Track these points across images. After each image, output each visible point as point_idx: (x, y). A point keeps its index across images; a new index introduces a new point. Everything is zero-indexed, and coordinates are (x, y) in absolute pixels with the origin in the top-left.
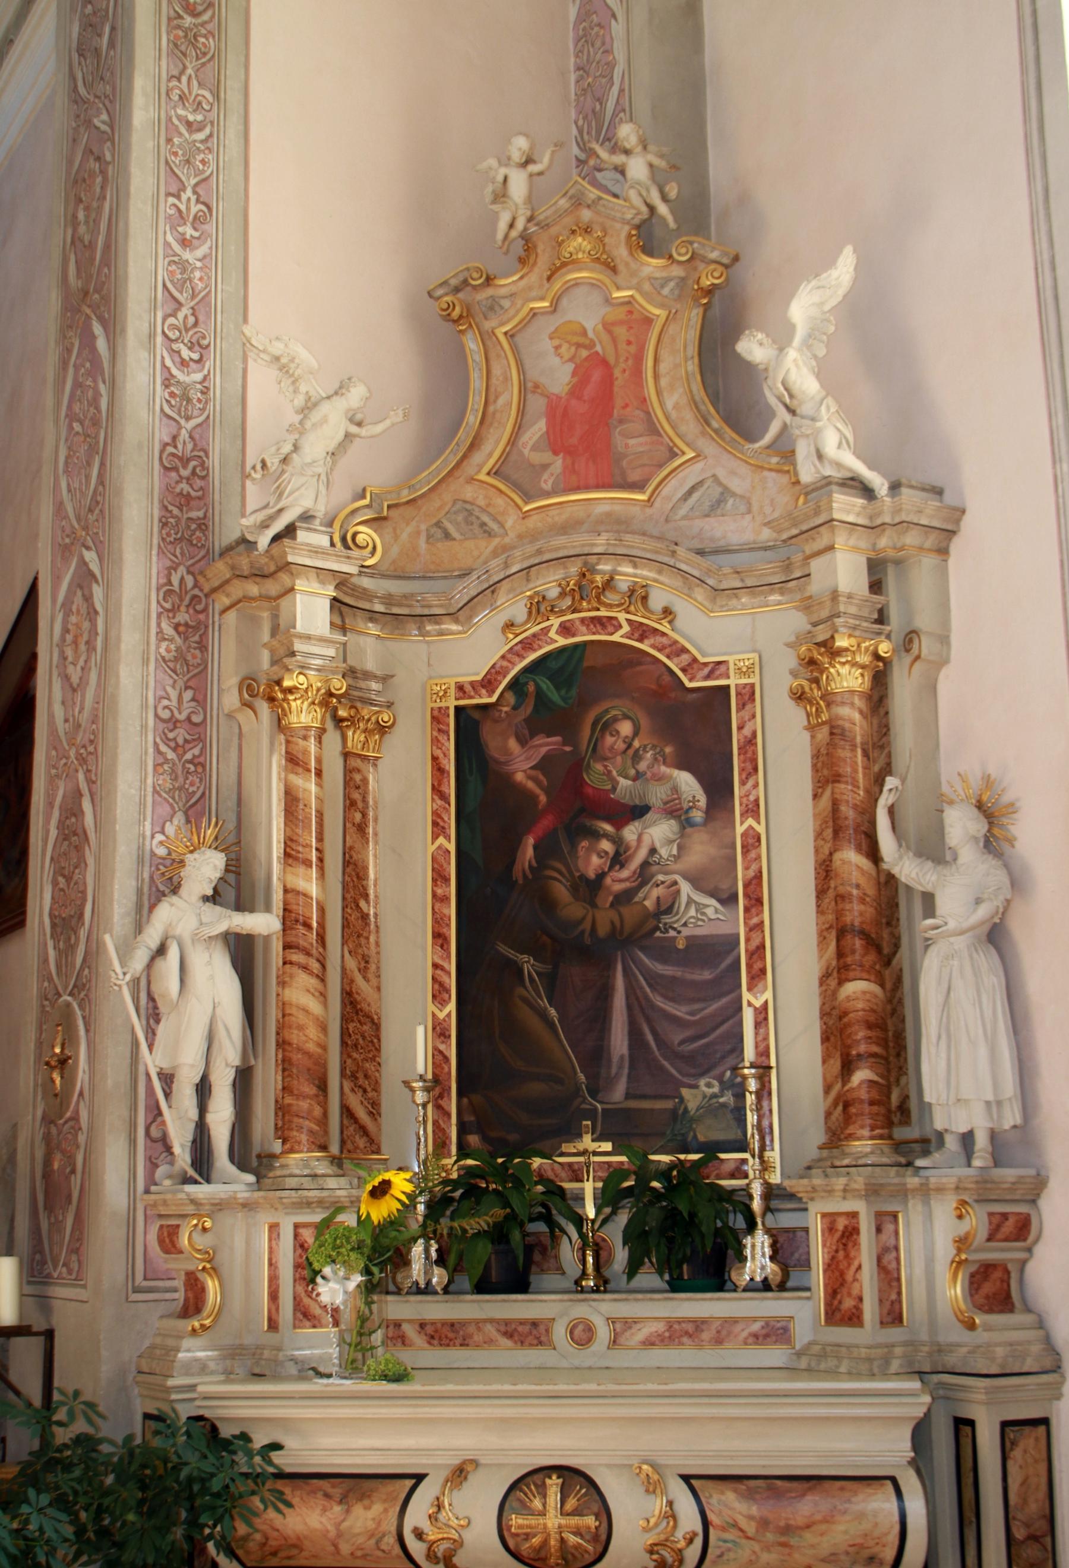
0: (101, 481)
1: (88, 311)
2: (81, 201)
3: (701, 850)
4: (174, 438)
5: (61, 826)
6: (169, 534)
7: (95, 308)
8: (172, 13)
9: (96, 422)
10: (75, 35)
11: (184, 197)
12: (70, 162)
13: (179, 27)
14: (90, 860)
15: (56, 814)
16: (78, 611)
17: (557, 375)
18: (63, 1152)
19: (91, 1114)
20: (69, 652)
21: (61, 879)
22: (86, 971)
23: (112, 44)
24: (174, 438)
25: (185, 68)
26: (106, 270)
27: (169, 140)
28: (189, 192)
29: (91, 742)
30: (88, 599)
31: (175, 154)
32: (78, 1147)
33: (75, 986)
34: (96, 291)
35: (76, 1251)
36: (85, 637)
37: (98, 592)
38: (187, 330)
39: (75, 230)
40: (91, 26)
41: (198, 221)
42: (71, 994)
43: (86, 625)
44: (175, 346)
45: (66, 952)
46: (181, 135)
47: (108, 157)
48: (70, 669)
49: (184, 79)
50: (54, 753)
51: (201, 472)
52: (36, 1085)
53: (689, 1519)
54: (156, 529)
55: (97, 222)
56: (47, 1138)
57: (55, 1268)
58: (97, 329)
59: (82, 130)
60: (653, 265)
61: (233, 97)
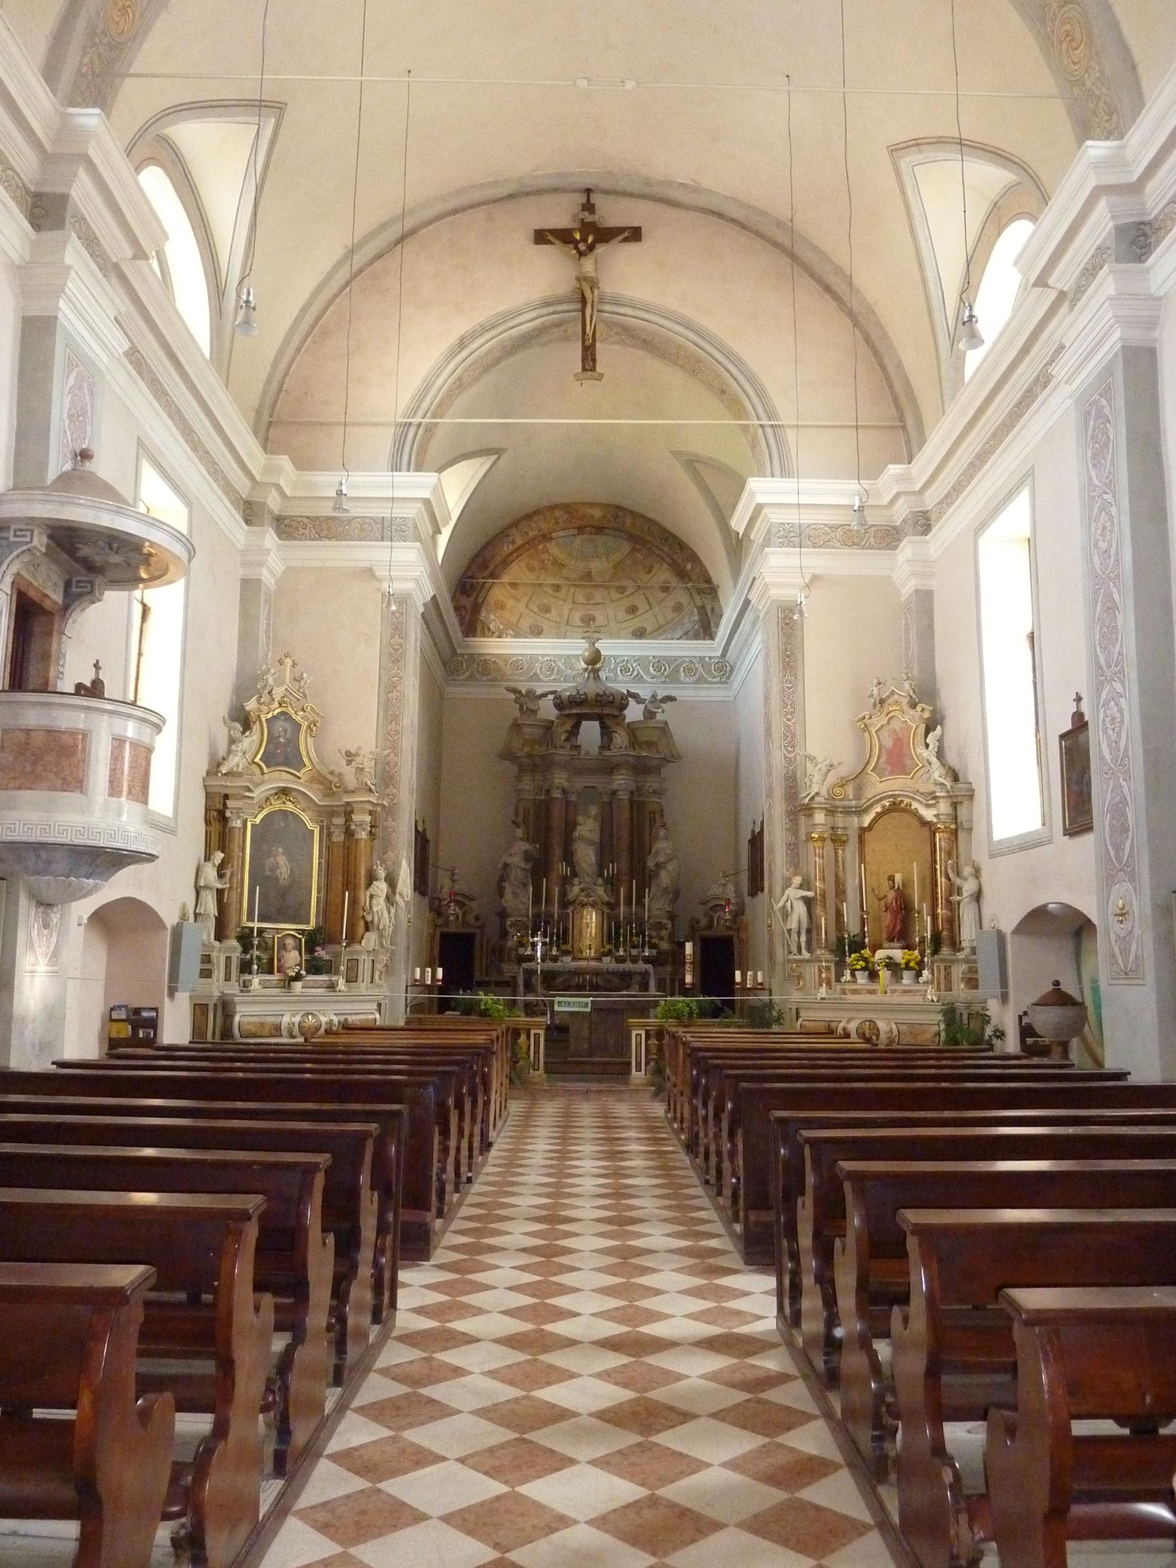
17: (888, 742)
41: (792, 713)
51: (795, 780)
53: (895, 1032)
60: (912, 712)
61: (800, 677)
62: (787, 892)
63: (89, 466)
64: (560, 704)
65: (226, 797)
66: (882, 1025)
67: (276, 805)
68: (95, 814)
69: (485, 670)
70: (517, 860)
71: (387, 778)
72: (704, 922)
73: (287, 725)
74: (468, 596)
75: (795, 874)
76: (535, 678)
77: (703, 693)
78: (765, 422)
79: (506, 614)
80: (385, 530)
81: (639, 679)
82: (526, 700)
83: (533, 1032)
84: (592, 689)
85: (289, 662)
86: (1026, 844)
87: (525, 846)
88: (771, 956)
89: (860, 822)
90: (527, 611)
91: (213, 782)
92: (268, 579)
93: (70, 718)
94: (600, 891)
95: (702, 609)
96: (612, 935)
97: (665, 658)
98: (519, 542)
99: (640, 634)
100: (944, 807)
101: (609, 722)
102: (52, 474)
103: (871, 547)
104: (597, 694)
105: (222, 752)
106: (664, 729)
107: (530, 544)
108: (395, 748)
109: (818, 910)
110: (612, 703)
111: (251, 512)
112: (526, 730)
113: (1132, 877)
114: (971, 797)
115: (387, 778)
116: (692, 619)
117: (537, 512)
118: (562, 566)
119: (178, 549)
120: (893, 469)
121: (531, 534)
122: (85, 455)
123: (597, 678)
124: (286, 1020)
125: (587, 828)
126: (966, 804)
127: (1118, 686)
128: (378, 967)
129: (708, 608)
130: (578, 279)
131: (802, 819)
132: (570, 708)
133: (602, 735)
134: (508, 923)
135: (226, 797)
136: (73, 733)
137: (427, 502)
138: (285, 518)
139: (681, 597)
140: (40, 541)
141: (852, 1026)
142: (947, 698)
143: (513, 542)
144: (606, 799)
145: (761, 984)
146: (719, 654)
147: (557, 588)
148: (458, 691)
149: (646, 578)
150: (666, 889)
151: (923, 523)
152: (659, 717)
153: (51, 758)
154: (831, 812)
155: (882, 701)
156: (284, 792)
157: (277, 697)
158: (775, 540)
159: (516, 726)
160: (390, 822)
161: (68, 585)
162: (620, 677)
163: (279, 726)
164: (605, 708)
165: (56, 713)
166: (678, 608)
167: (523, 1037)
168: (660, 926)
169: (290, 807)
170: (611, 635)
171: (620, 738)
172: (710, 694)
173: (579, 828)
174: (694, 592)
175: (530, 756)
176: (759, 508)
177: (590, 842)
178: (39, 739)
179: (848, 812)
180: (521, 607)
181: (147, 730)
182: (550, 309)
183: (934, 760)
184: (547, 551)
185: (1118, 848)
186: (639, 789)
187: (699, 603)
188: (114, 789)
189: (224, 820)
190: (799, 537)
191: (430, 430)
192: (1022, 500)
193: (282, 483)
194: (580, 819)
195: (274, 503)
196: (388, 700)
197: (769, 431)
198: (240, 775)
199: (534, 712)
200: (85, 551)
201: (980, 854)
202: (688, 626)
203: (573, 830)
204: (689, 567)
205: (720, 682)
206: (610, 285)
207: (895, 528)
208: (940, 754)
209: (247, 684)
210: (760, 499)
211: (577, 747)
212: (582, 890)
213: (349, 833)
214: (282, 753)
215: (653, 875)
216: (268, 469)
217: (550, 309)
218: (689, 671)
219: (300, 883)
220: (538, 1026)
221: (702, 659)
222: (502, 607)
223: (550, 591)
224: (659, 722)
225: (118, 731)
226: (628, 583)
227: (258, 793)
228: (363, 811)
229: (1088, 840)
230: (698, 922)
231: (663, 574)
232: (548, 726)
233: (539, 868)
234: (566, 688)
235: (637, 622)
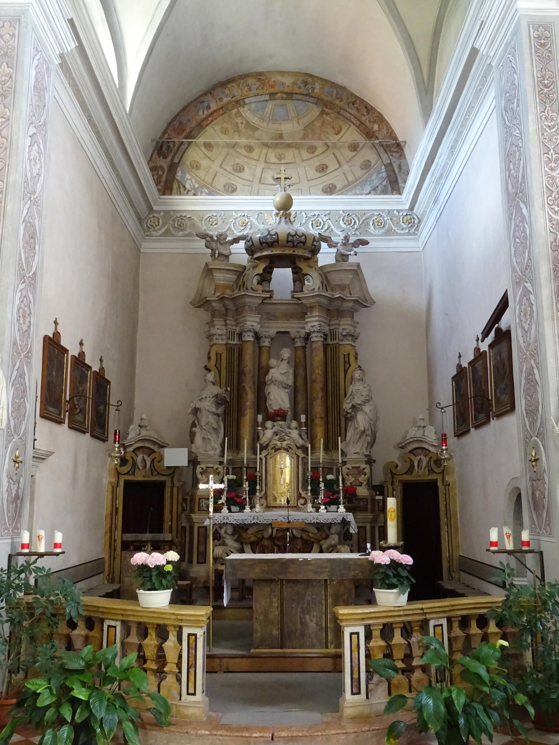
0: (529, 259)
1: (518, 199)
2: (511, 162)
4: (555, 239)
5: (526, 378)
6: (557, 274)
7: (521, 198)
8: (540, 90)
9: (525, 238)
10: (503, 104)
11: (550, 153)
12: (506, 149)
13: (542, 93)
14: (539, 390)
15: (524, 374)
16: (525, 304)
18: (540, 491)
19: (549, 477)
20: (523, 319)
21: (528, 397)
22: (542, 429)
23: (518, 106)
24: (555, 239)
25: (546, 107)
26: (524, 184)
27: (543, 134)
28: (552, 151)
29: (535, 349)
30: (529, 300)
31: (545, 139)
32: (545, 489)
33: (538, 434)
34: (520, 192)
35: (549, 525)
36: (529, 313)
37: (532, 297)
38: (556, 200)
39: (509, 172)
40: (509, 101)
42: (537, 436)
43: (529, 309)
44: (552, 207)
45: (533, 423)
46: (547, 131)
47: (521, 145)
48: (524, 325)
49: (546, 111)
50: (520, 354)
52: (526, 467)
54: (552, 273)
55: (518, 168)
56: (532, 486)
57: (541, 530)
58: (522, 205)
59: (509, 137)
64: (250, 250)
69: (179, 224)
70: (208, 405)
72: (402, 467)
74: (165, 157)
77: (393, 244)
82: (217, 244)
83: (186, 632)
84: (283, 229)
87: (216, 390)
90: (221, 170)
94: (295, 434)
95: (389, 167)
98: (214, 107)
99: (330, 190)
101: (302, 265)
104: (289, 234)
106: (357, 271)
107: (224, 109)
110: (304, 243)
112: (218, 275)
116: (379, 177)
117: (230, 81)
121: (225, 100)
123: (287, 216)
125: (280, 372)
129: (395, 166)
132: (261, 250)
133: (295, 281)
134: (199, 470)
139: (368, 154)
143: (208, 107)
144: (299, 344)
145: (528, 544)
146: (407, 207)
149: (334, 139)
150: (364, 432)
152: (352, 259)
159: (208, 271)
166: (366, 165)
167: (172, 637)
168: (359, 471)
171: (312, 283)
172: (400, 244)
173: (272, 371)
174: (381, 150)
175: (222, 299)
177: (286, 387)
180: (215, 166)
184: (241, 115)
186: (333, 334)
187: (387, 161)
194: (273, 362)
199: (227, 257)
202: (376, 182)
203: (267, 372)
204: (376, 127)
205: (409, 234)
212: (276, 434)
215: (349, 418)
218: (380, 224)
221: (389, 212)
222: (198, 167)
223: (243, 151)
224: (352, 265)
226: (316, 143)
230: (397, 466)
231: (351, 134)
232: (240, 272)
233: (230, 411)
235: (327, 180)
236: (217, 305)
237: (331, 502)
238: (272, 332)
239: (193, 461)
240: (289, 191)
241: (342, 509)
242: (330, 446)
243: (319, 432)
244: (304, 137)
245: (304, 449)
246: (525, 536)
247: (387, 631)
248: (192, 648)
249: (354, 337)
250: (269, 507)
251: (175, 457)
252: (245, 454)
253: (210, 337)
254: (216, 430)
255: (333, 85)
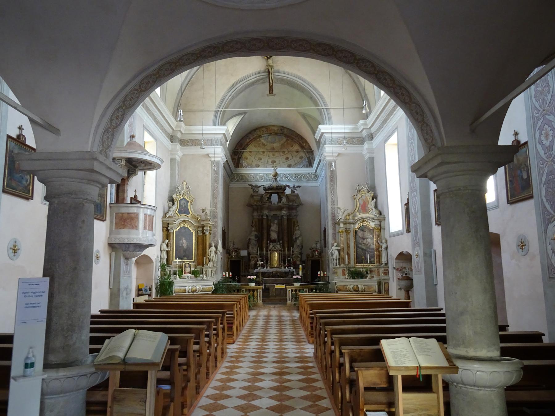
3: (372, 241)
62: (333, 248)
63: (134, 139)
64: (265, 189)
65: (168, 224)
66: (359, 286)
67: (182, 225)
68: (140, 235)
69: (241, 178)
70: (253, 237)
71: (214, 216)
72: (311, 255)
73: (185, 202)
75: (335, 242)
76: (257, 180)
78: (324, 107)
79: (248, 161)
80: (212, 143)
81: (289, 180)
82: (255, 188)
84: (275, 184)
85: (185, 183)
86: (398, 234)
87: (255, 233)
88: (329, 267)
89: (354, 227)
91: (164, 219)
92: (178, 158)
93: (133, 209)
94: (279, 246)
95: (309, 158)
96: (284, 260)
97: (298, 174)
98: (252, 138)
99: (290, 166)
100: (377, 222)
101: (280, 194)
102: (125, 143)
103: (356, 144)
105: (166, 210)
106: (297, 196)
107: (255, 139)
108: (216, 207)
109: (342, 253)
111: (172, 139)
112: (255, 197)
113: (419, 246)
114: (385, 219)
115: (214, 216)
116: (305, 161)
118: (265, 145)
119: (159, 162)
120: (362, 122)
122: (133, 137)
123: (276, 181)
124: (187, 288)
126: (383, 221)
127: (415, 193)
128: (213, 272)
130: (267, 66)
131: (337, 226)
135: (168, 224)
136: (134, 213)
137: (224, 134)
138: (182, 139)
139: (302, 154)
140: (123, 163)
141: (352, 286)
142: (379, 191)
144: (280, 218)
147: (264, 152)
148: (233, 185)
149: (291, 148)
151: (371, 137)
152: (296, 192)
153: (129, 220)
154: (345, 223)
155: (359, 191)
156: (184, 221)
157: (182, 194)
158: (327, 143)
159: (252, 196)
160: (215, 229)
161: (128, 171)
162: (284, 180)
163: (183, 202)
164: (280, 190)
165: (130, 208)
166: (301, 158)
167: (256, 292)
168: (297, 257)
169: (186, 226)
170: (280, 167)
171: (284, 200)
172: (312, 184)
175: (256, 205)
176: (322, 134)
177: (276, 232)
178: (126, 215)
179: (350, 223)
180: (252, 158)
181: (153, 211)
182: (259, 75)
183: (374, 209)
185: (416, 237)
186: (290, 215)
188: (145, 228)
189: (168, 230)
190: (333, 142)
191: (224, 112)
192: (395, 135)
193: (182, 130)
194: (272, 224)
195: (179, 135)
196: (214, 193)
197: (325, 110)
198: (172, 217)
200: (134, 163)
201: (387, 237)
202: (305, 163)
206: (276, 68)
207: (363, 138)
208: (376, 207)
209: (173, 190)
210: (322, 131)
211: (271, 202)
213: (203, 233)
214: (184, 210)
215: (295, 241)
216: (177, 126)
217: (259, 75)
218: (305, 177)
219: (189, 249)
220: (260, 289)
222: (247, 159)
223: (261, 153)
225: (146, 213)
226: (286, 150)
227: (177, 222)
228: (207, 226)
229: (410, 234)
231: (296, 147)
232: (262, 196)
233: (260, 240)
234: (267, 184)
236: (255, 207)
237: (289, 266)
238: (272, 214)
239: (249, 254)
240: (277, 170)
241: (292, 268)
242: (289, 250)
243: (286, 245)
244: (281, 148)
245: (282, 251)
246: (325, 273)
247: (296, 291)
248: (260, 293)
249: (296, 216)
250: (271, 268)
251: (244, 253)
252: (264, 252)
253: (253, 216)
254: (256, 245)
255: (291, 130)
